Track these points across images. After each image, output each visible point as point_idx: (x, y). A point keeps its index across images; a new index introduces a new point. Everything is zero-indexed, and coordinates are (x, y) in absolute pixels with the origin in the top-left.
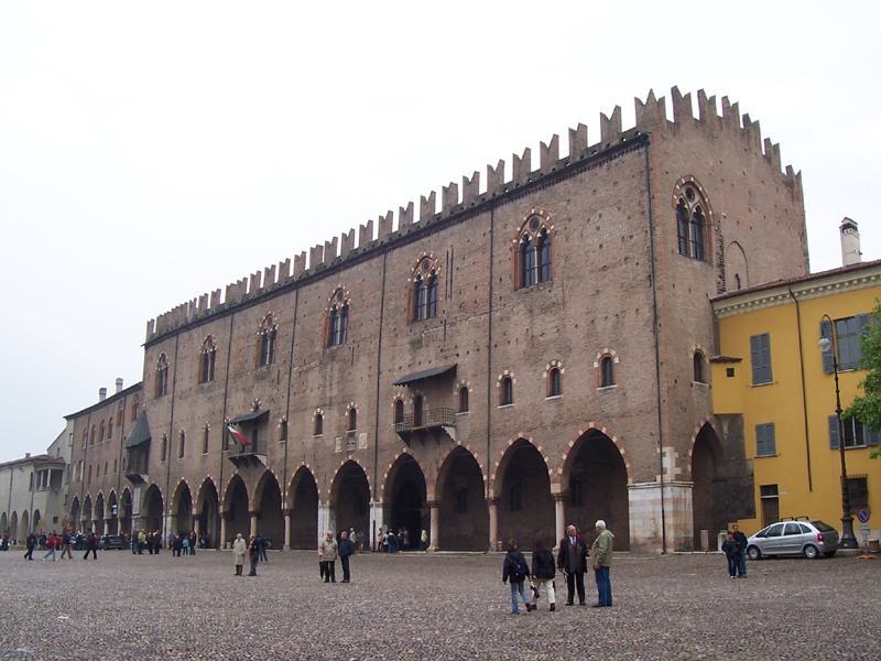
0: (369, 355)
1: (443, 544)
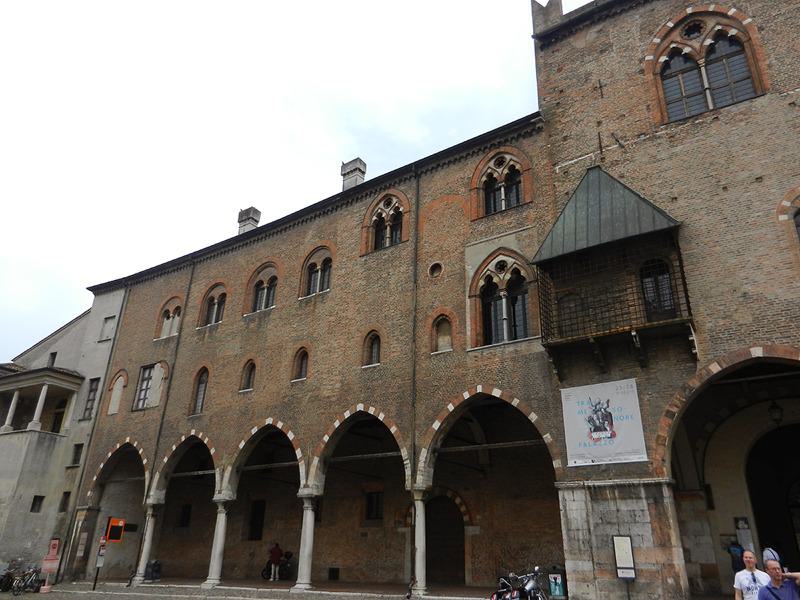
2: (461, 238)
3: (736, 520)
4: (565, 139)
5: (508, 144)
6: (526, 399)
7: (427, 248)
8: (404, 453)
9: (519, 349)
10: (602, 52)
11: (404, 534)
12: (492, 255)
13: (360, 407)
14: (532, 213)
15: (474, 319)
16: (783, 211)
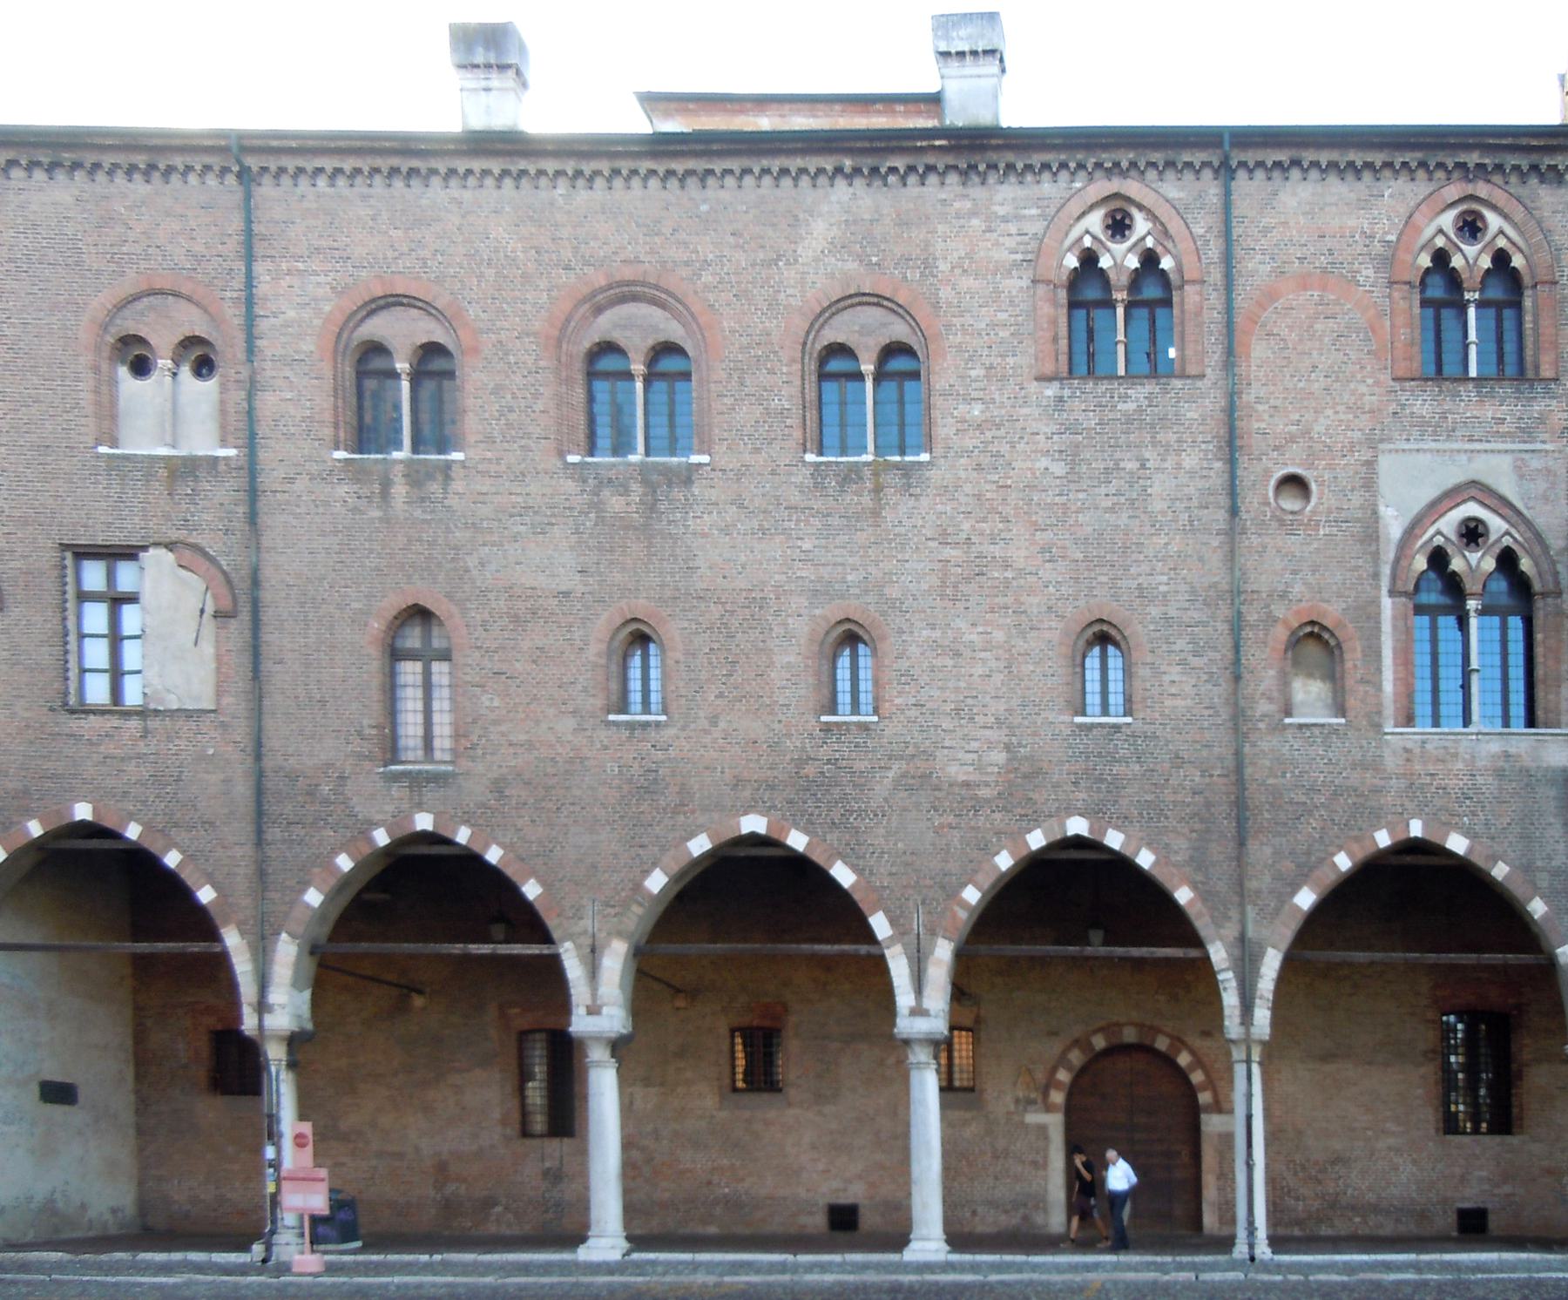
2: (1364, 422)
5: (1497, 179)
6: (1526, 869)
8: (1218, 954)
9: (1512, 750)
11: (1042, 1130)
12: (1453, 496)
13: (1077, 826)
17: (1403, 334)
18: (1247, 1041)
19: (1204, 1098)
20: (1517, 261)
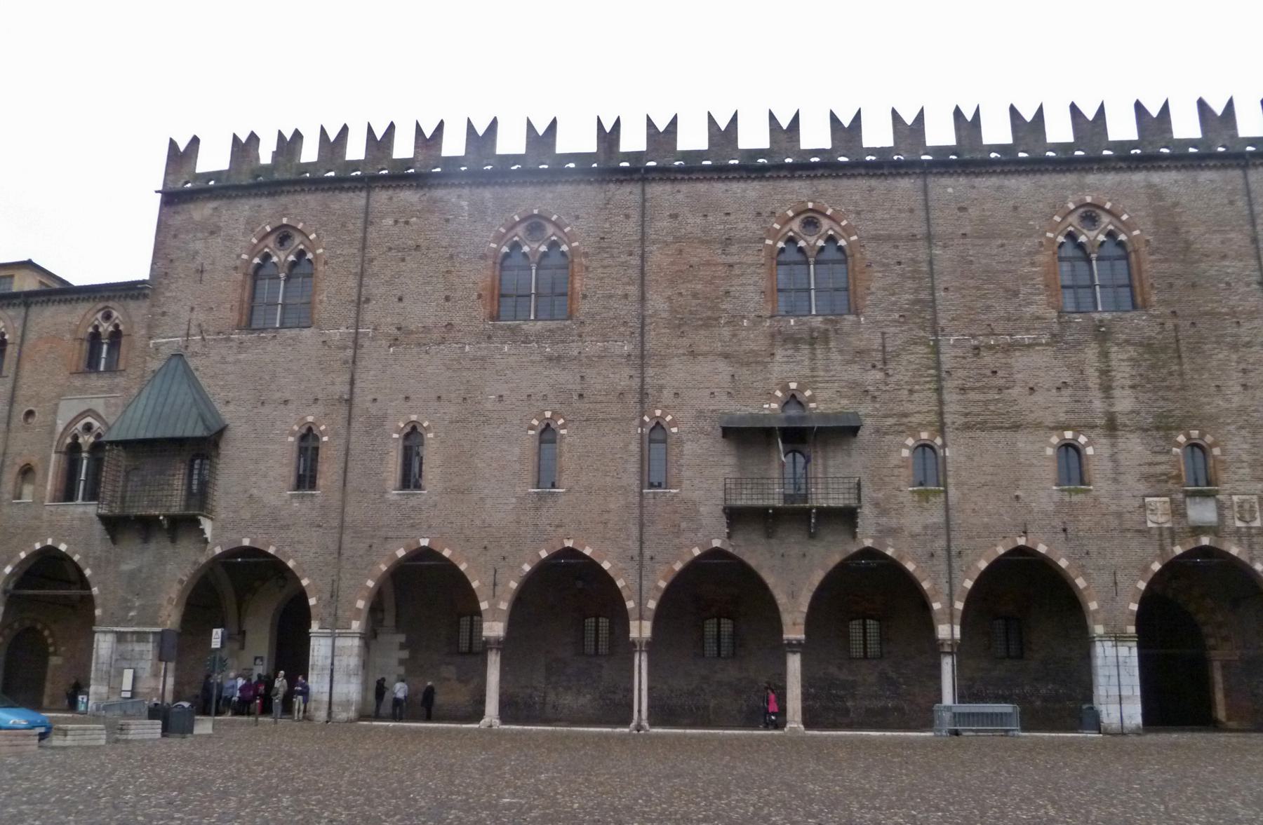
0: (1234, 347)
1: (663, 713)
3: (256, 658)
4: (164, 314)
6: (85, 556)
7: (23, 392)
10: (212, 233)
14: (120, 380)
15: (56, 474)
16: (292, 434)
17: (76, 357)
18: (641, 652)
19: (51, 649)
20: (121, 328)
